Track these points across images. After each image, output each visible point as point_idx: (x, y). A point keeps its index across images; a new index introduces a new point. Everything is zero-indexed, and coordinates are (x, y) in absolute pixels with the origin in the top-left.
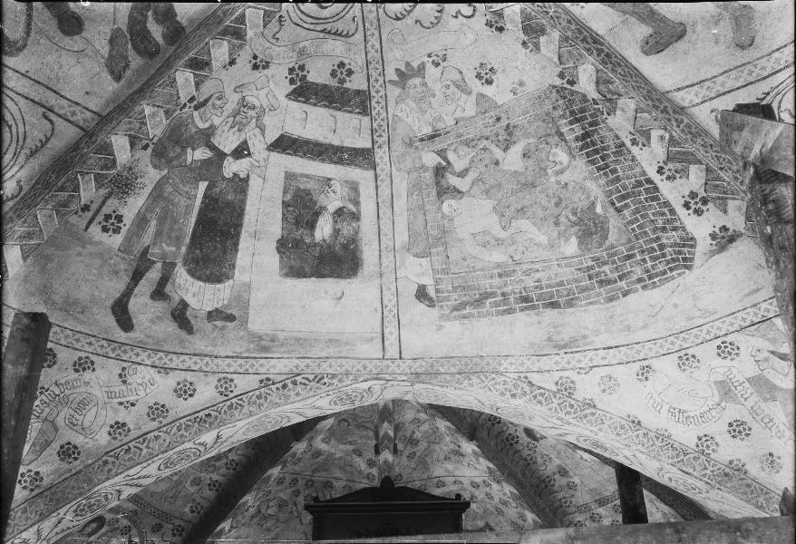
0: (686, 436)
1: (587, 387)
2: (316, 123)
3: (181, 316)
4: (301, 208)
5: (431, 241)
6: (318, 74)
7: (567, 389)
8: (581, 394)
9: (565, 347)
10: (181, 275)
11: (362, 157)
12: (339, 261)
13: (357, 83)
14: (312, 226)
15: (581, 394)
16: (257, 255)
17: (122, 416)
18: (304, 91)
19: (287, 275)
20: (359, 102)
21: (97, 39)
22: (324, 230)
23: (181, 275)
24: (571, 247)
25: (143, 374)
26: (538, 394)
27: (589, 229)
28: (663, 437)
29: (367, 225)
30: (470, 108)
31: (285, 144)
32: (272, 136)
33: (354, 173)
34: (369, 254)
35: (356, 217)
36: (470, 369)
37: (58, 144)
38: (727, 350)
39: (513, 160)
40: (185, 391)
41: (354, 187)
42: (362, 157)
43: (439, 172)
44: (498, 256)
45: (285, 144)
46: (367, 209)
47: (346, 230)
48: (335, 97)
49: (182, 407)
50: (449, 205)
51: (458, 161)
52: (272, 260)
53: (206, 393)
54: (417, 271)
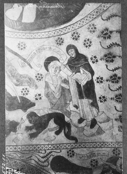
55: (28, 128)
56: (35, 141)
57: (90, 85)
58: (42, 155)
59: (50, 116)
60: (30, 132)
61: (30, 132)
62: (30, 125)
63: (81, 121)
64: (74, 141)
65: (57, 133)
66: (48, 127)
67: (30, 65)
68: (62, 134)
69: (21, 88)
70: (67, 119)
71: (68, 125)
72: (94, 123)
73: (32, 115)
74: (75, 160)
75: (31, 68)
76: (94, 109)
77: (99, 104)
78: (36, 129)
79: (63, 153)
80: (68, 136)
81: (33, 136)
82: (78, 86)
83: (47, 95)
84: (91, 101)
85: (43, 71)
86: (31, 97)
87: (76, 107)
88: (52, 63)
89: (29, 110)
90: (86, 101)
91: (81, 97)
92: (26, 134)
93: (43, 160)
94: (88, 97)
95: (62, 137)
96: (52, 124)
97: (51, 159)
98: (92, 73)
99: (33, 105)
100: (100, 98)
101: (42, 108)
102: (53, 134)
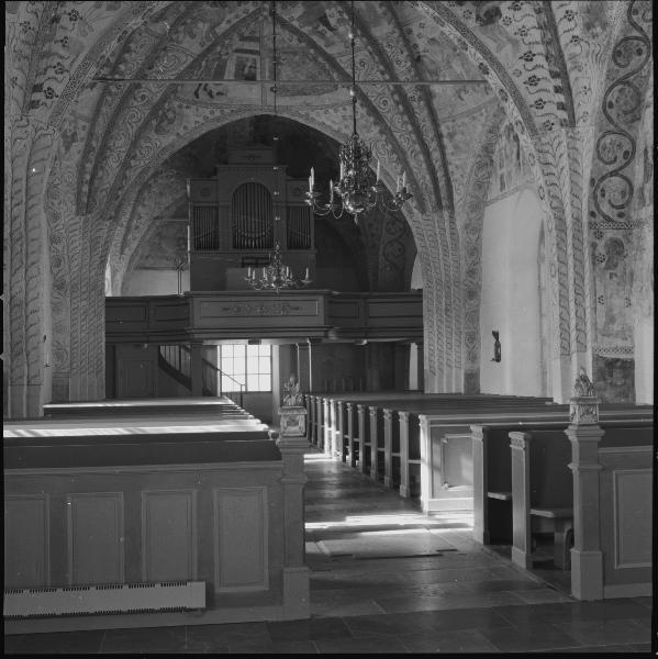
0: (336, 127)
1: (313, 115)
2: (248, 46)
3: (210, 94)
4: (240, 66)
5: (275, 75)
6: (247, 34)
7: (307, 115)
11: (257, 53)
12: (251, 78)
13: (257, 35)
14: (243, 70)
17: (197, 119)
18: (243, 39)
20: (257, 40)
22: (246, 70)
25: (200, 110)
26: (302, 116)
28: (330, 127)
29: (258, 71)
31: (237, 51)
33: (255, 57)
34: (258, 78)
37: (188, 62)
38: (345, 109)
40: (212, 113)
41: (255, 60)
42: (257, 53)
45: (237, 51)
46: (258, 65)
49: (211, 117)
53: (218, 113)
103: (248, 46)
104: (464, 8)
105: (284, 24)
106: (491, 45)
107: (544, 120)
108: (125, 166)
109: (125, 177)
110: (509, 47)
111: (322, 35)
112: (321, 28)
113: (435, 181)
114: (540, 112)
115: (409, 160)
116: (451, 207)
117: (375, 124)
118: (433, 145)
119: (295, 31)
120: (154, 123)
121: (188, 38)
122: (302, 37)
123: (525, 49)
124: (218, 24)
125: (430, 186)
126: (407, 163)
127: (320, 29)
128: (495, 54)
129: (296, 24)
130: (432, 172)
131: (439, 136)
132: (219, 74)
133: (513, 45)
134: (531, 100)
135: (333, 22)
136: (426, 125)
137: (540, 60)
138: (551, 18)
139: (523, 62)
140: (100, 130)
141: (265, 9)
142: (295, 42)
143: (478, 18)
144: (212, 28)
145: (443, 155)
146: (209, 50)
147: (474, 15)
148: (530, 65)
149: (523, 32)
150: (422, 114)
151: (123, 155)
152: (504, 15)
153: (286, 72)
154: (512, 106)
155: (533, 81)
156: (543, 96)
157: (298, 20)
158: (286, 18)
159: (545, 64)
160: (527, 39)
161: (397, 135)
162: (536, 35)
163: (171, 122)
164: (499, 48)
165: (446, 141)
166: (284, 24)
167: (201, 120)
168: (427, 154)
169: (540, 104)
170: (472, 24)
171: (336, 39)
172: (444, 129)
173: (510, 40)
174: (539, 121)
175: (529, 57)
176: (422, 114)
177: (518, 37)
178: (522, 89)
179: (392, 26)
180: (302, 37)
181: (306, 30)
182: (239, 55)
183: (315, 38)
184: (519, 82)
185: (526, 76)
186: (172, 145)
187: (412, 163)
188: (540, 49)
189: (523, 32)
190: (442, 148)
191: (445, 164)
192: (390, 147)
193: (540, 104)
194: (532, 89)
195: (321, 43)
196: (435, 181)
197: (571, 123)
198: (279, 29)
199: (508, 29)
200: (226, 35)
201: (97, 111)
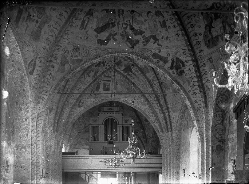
2: (106, 79)
4: (105, 85)
7: (126, 101)
8: (127, 101)
9: (126, 98)
10: (95, 91)
14: (106, 86)
15: (127, 101)
16: (101, 89)
18: (105, 76)
19: (104, 91)
20: (110, 77)
21: (91, 77)
22: (107, 87)
23: (95, 91)
24: (127, 90)
27: (128, 89)
30: (119, 79)
31: (104, 80)
32: (103, 80)
33: (110, 82)
34: (110, 89)
35: (109, 86)
36: (119, 99)
39: (122, 83)
40: (96, 100)
41: (109, 83)
43: (117, 83)
44: (121, 90)
45: (104, 80)
46: (110, 85)
47: (109, 87)
48: (108, 77)
50: (117, 85)
51: (118, 82)
52: (102, 89)
54: (114, 91)
55: (143, 42)
56: (146, 47)
57: (164, 21)
58: (149, 52)
59: (151, 37)
60: (144, 43)
61: (144, 43)
62: (144, 41)
63: (162, 38)
64: (160, 46)
65: (154, 43)
66: (150, 41)
67: (141, 16)
68: (156, 44)
69: (139, 26)
70: (157, 37)
71: (158, 40)
72: (167, 38)
73: (144, 37)
74: (161, 54)
75: (142, 17)
76: (167, 32)
77: (169, 30)
78: (146, 42)
79: (157, 52)
80: (158, 45)
81: (145, 45)
82: (160, 23)
83: (149, 28)
84: (165, 29)
85: (147, 18)
86: (143, 29)
87: (160, 32)
88: (149, 14)
89: (143, 35)
90: (164, 29)
91: (162, 27)
92: (142, 45)
93: (149, 54)
94: (164, 27)
95: (156, 45)
96: (152, 40)
97: (152, 54)
98: (164, 17)
99: (144, 32)
100: (168, 27)
101: (148, 34)
102: (153, 43)
103: (106, 79)
104: (172, 70)
105: (119, 72)
106: (181, 83)
107: (198, 106)
108: (69, 117)
109: (68, 121)
110: (187, 83)
111: (130, 75)
112: (130, 73)
113: (166, 122)
114: (196, 104)
115: (158, 116)
116: (171, 131)
117: (147, 104)
118: (166, 111)
119: (122, 74)
120: (77, 104)
121: (88, 77)
122: (124, 76)
123: (192, 83)
124: (98, 72)
125: (165, 124)
126: (158, 117)
127: (129, 74)
128: (183, 85)
129: (122, 72)
130: (165, 119)
131: (168, 108)
132: (98, 89)
133: (189, 82)
134: (193, 100)
135: (134, 71)
136: (163, 104)
137: (197, 87)
138: (200, 73)
139: (191, 87)
140: (60, 106)
141: (112, 68)
142: (122, 78)
143: (177, 73)
144: (96, 73)
145: (169, 114)
146: (94, 81)
147: (176, 73)
148: (193, 89)
149: (192, 78)
150: (162, 101)
151: (68, 114)
152: (185, 73)
153: (119, 87)
154: (188, 102)
155: (195, 94)
156: (198, 99)
157: (123, 71)
158: (119, 70)
159: (198, 89)
160: (193, 80)
161: (154, 108)
162: (196, 79)
163: (83, 103)
164: (184, 83)
165: (170, 110)
166: (119, 72)
167: (92, 103)
168: (164, 113)
169: (197, 101)
170: (175, 75)
171: (135, 77)
172: (169, 106)
173: (187, 81)
174: (196, 106)
175: (193, 86)
176: (162, 101)
177: (190, 80)
178: (191, 96)
179: (152, 73)
180: (124, 76)
181: (125, 74)
182: (104, 82)
183: (128, 77)
184: (190, 94)
185: (192, 92)
186: (83, 111)
187: (159, 117)
188: (197, 83)
189: (192, 78)
190: (169, 112)
191: (170, 117)
192: (152, 111)
193: (197, 101)
194: (194, 96)
195: (130, 78)
196: (166, 122)
197: (207, 107)
198: (116, 74)
199: (187, 77)
200: (100, 76)
201: (59, 101)
